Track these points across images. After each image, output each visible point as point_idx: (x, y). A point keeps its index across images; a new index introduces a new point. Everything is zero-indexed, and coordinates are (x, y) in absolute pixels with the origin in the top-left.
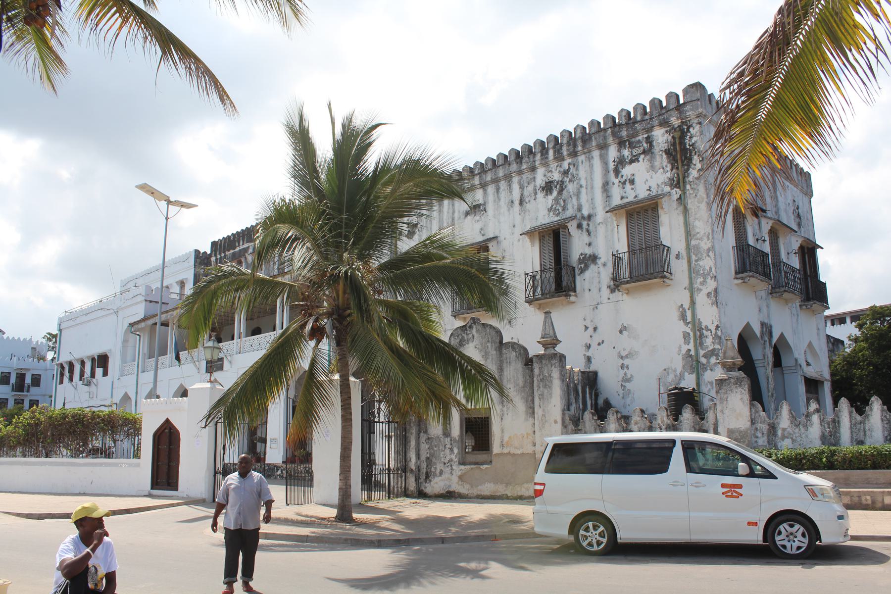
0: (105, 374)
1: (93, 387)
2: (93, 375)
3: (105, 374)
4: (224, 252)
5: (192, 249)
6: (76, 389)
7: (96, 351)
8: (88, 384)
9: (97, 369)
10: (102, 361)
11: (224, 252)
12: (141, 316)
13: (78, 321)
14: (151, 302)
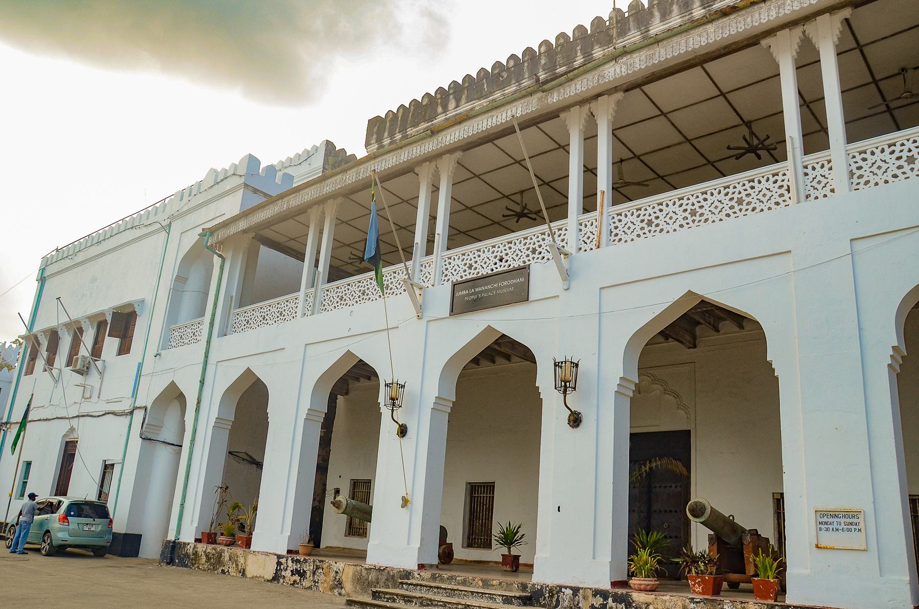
0: (124, 349)
1: (93, 379)
2: (96, 352)
3: (124, 349)
4: (403, 130)
5: (319, 141)
6: (57, 381)
7: (106, 303)
8: (84, 371)
9: (108, 340)
10: (122, 324)
11: (403, 130)
12: (236, 211)
13: (80, 257)
14: (256, 191)
